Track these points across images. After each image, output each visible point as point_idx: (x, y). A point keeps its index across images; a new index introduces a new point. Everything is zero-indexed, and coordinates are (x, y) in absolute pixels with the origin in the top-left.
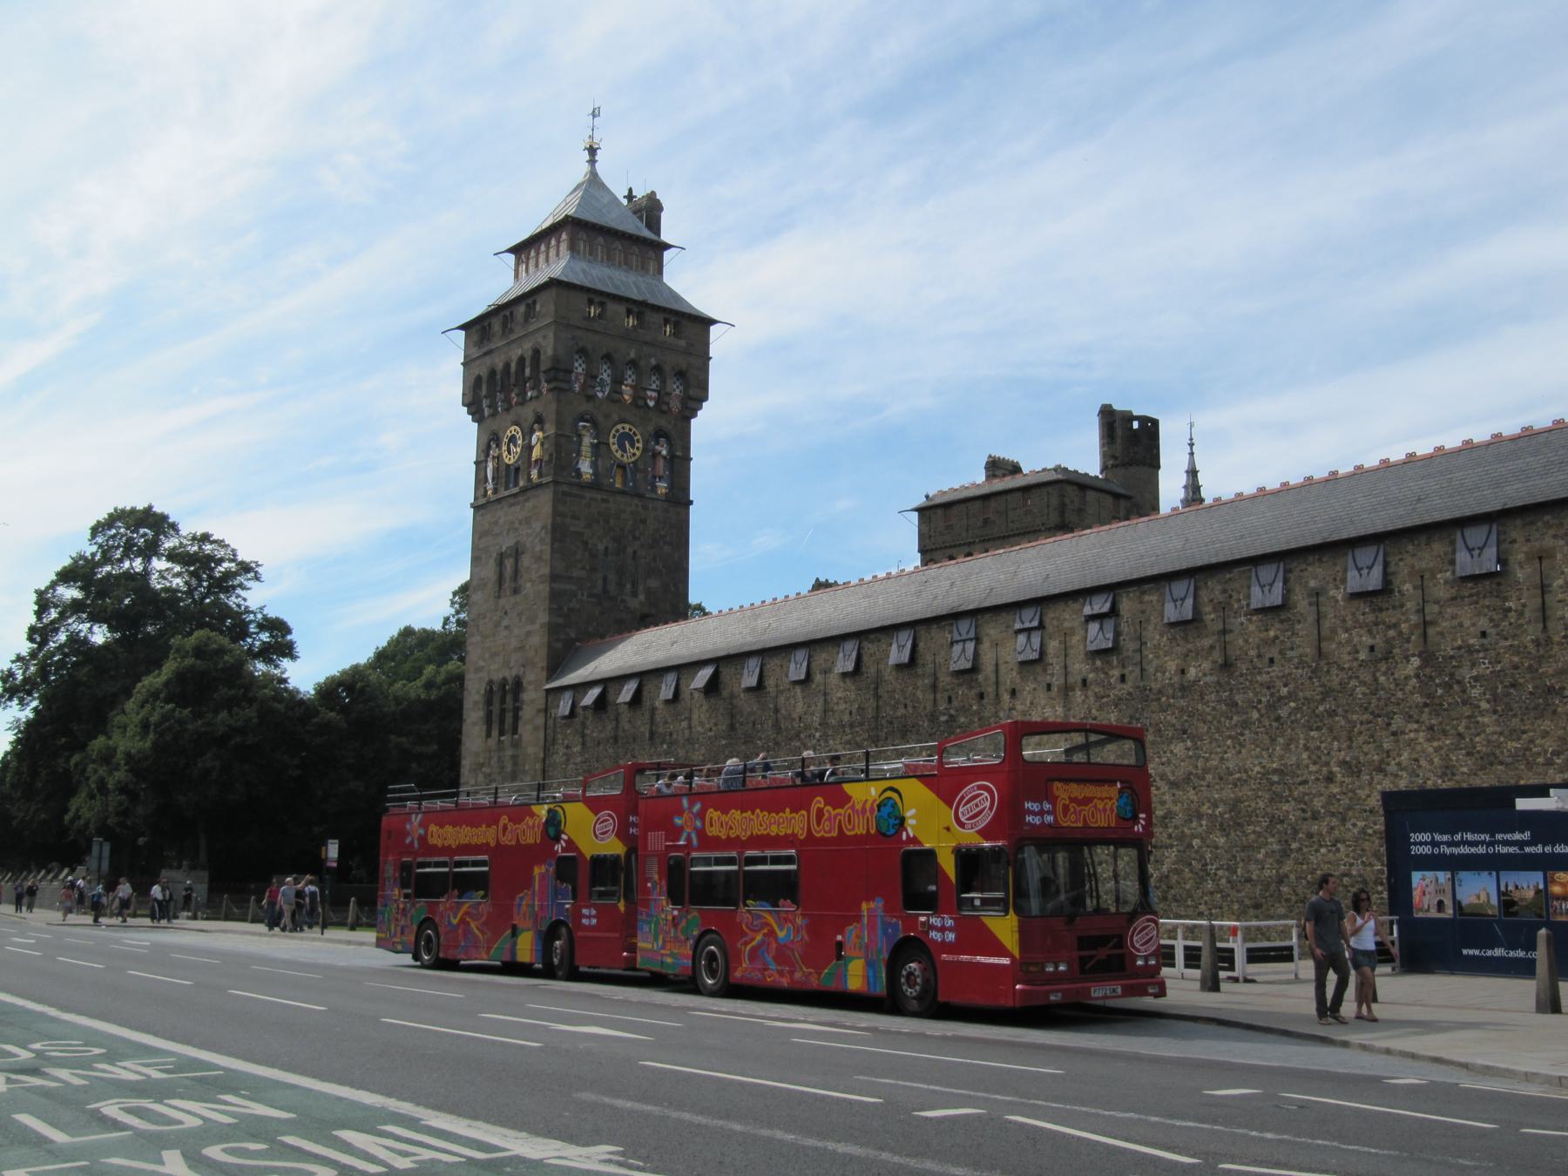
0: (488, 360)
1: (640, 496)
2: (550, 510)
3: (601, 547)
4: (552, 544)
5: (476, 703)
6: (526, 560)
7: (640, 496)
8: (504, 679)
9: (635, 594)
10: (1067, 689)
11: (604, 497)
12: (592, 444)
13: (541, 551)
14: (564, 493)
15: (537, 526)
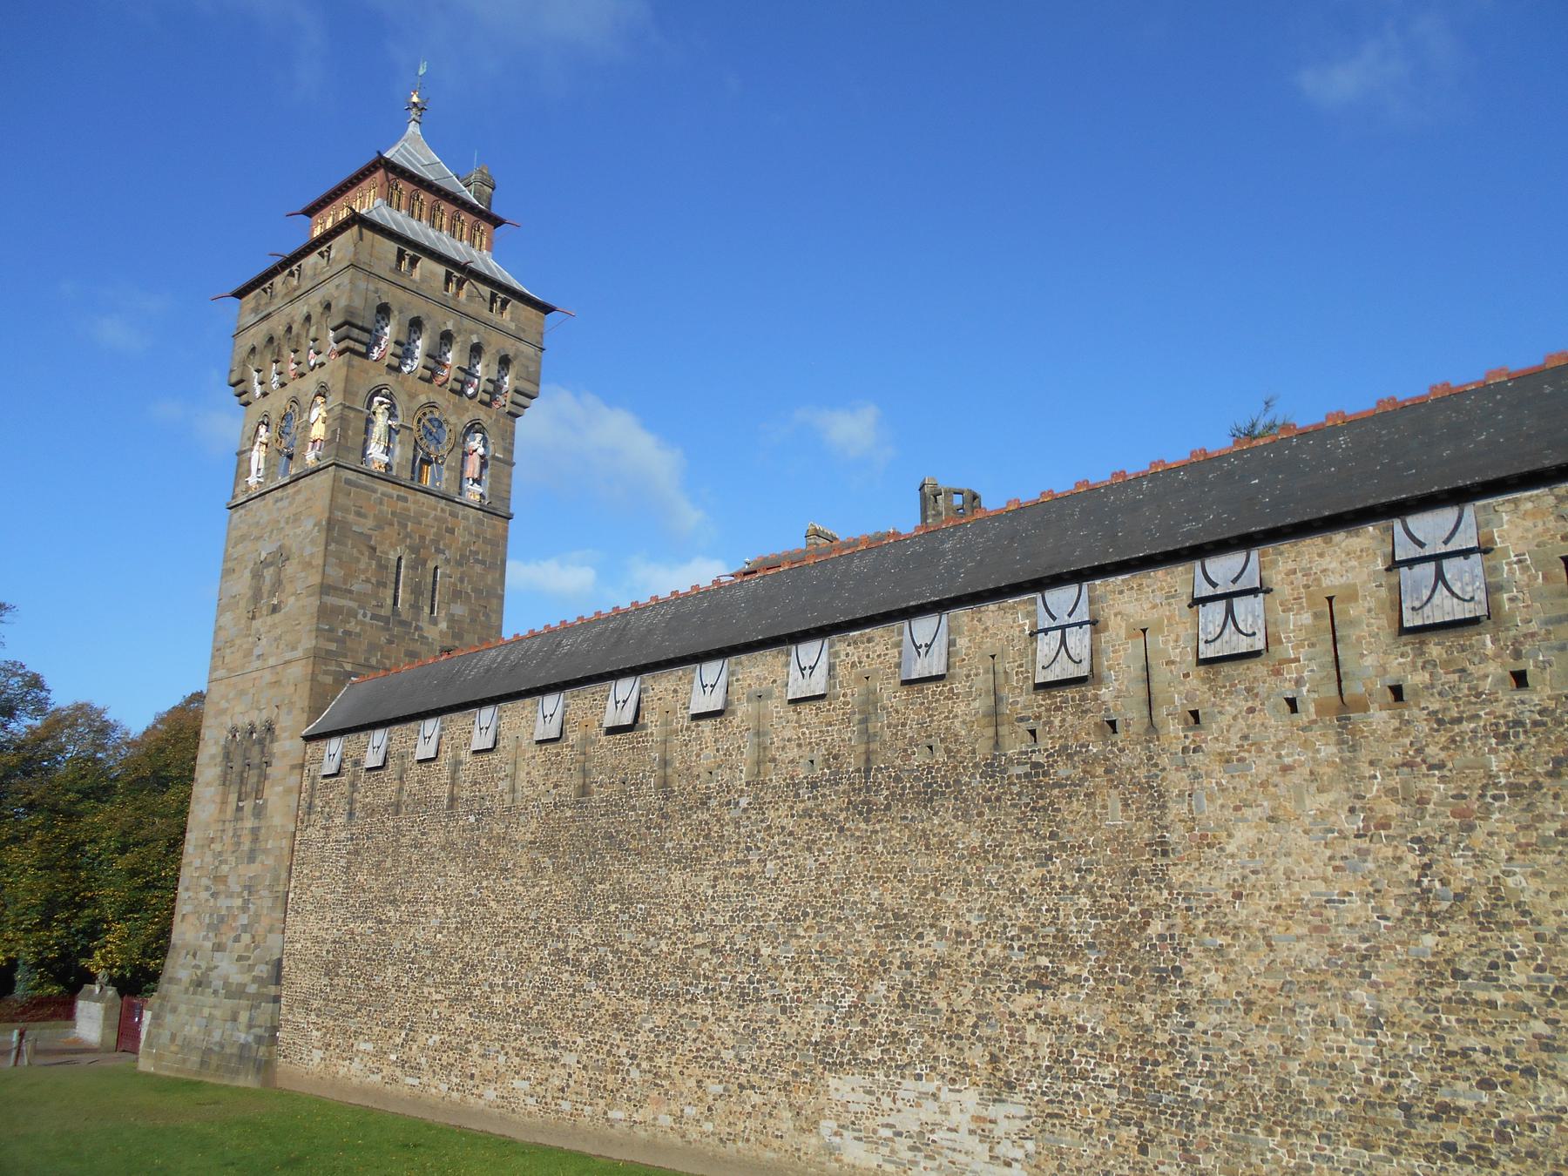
0: (264, 326)
1: (450, 500)
2: (327, 502)
3: (393, 557)
4: (327, 544)
5: (213, 757)
6: (291, 569)
7: (450, 500)
8: (252, 725)
9: (434, 622)
10: (1344, 709)
11: (402, 494)
12: (390, 426)
13: (312, 555)
14: (348, 482)
15: (308, 525)
